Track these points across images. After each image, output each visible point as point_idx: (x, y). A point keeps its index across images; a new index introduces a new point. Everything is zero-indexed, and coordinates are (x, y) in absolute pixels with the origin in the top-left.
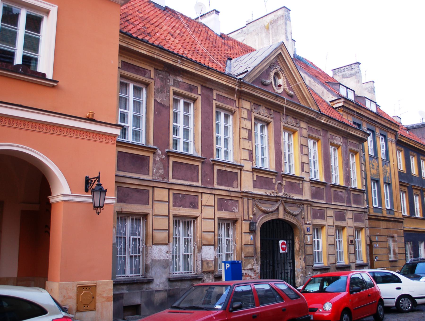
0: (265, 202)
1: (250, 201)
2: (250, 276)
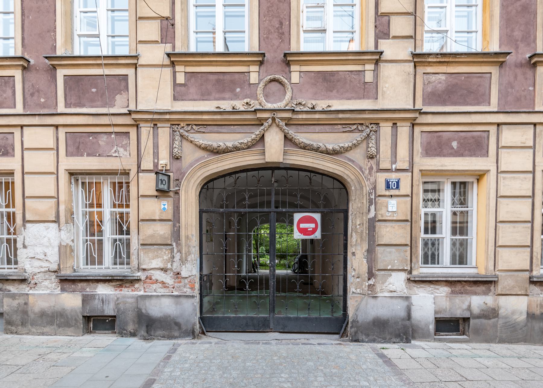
0: (215, 128)
1: (164, 133)
2: (163, 283)
